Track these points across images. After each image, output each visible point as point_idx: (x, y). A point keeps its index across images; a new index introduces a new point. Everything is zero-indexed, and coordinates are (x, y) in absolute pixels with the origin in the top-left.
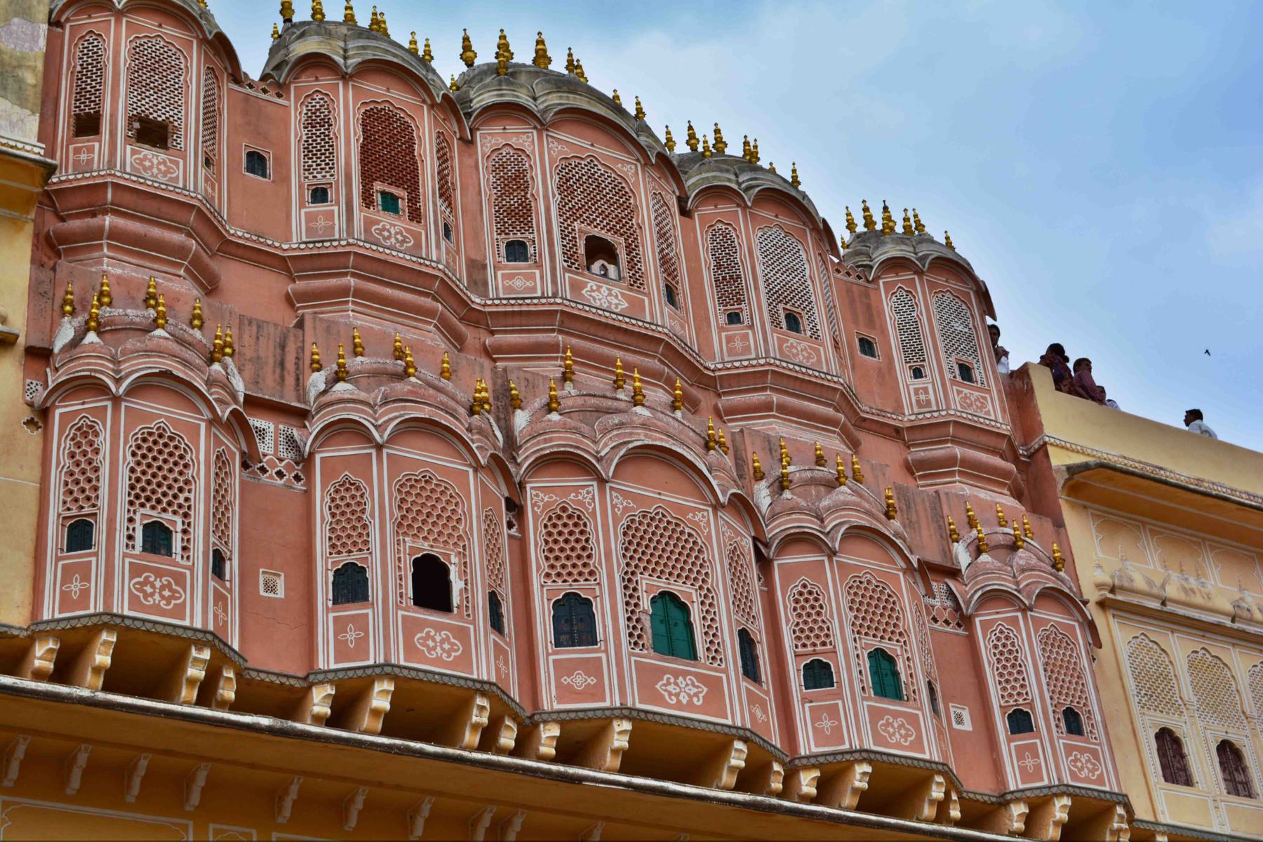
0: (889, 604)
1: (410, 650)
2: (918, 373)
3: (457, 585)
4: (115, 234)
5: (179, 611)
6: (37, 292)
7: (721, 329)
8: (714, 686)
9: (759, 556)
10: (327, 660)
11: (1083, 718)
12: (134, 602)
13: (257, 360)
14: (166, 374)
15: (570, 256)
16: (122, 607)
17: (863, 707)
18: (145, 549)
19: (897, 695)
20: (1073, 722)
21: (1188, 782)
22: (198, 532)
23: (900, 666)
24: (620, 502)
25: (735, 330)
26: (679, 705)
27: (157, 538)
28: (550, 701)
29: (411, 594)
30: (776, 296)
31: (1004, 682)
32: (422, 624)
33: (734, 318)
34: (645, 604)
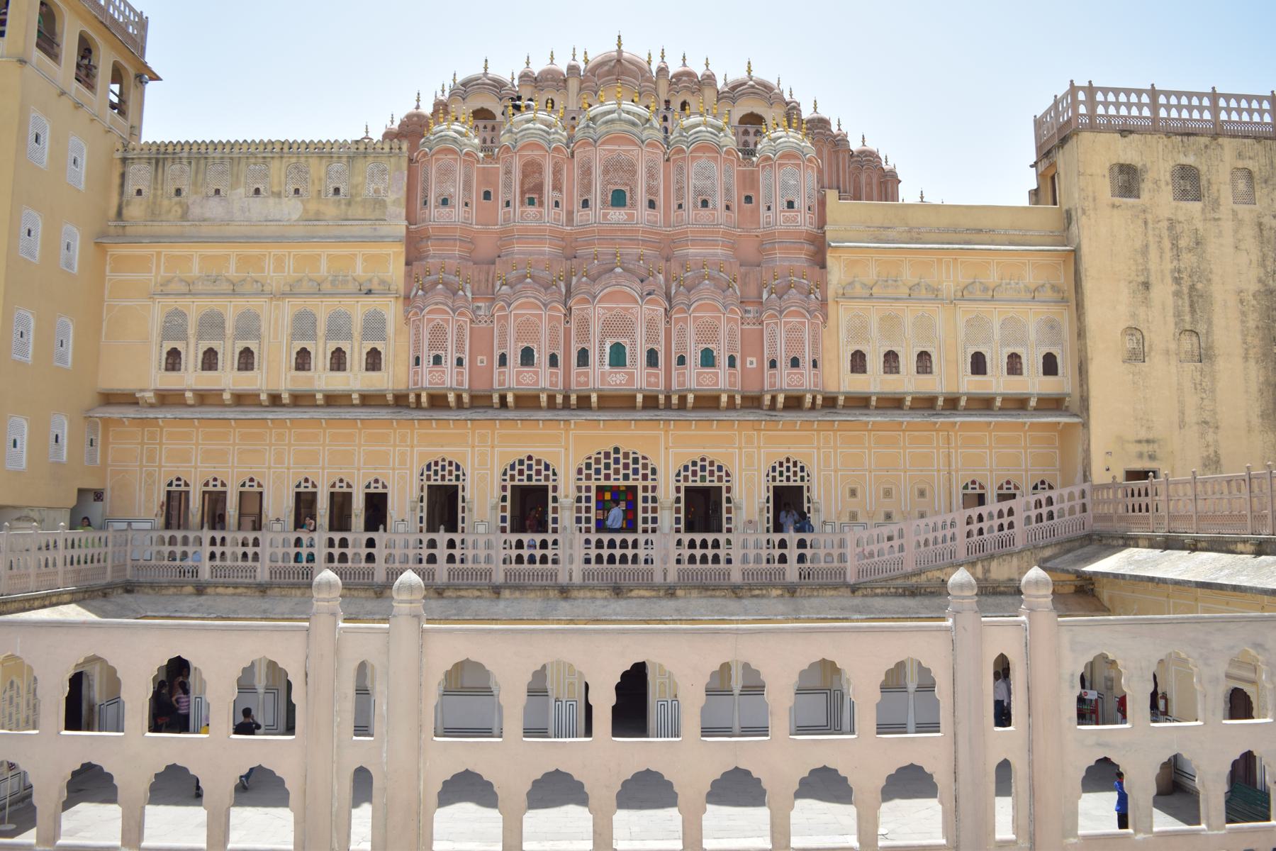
0: (715, 329)
1: (518, 382)
2: (769, 208)
3: (536, 355)
5: (443, 383)
6: (408, 275)
8: (631, 375)
10: (496, 386)
12: (430, 383)
13: (479, 281)
15: (604, 202)
17: (694, 376)
19: (713, 365)
20: (795, 363)
21: (865, 372)
24: (602, 311)
25: (680, 211)
27: (437, 360)
28: (574, 386)
30: (699, 192)
31: (770, 347)
33: (680, 206)
34: (608, 350)
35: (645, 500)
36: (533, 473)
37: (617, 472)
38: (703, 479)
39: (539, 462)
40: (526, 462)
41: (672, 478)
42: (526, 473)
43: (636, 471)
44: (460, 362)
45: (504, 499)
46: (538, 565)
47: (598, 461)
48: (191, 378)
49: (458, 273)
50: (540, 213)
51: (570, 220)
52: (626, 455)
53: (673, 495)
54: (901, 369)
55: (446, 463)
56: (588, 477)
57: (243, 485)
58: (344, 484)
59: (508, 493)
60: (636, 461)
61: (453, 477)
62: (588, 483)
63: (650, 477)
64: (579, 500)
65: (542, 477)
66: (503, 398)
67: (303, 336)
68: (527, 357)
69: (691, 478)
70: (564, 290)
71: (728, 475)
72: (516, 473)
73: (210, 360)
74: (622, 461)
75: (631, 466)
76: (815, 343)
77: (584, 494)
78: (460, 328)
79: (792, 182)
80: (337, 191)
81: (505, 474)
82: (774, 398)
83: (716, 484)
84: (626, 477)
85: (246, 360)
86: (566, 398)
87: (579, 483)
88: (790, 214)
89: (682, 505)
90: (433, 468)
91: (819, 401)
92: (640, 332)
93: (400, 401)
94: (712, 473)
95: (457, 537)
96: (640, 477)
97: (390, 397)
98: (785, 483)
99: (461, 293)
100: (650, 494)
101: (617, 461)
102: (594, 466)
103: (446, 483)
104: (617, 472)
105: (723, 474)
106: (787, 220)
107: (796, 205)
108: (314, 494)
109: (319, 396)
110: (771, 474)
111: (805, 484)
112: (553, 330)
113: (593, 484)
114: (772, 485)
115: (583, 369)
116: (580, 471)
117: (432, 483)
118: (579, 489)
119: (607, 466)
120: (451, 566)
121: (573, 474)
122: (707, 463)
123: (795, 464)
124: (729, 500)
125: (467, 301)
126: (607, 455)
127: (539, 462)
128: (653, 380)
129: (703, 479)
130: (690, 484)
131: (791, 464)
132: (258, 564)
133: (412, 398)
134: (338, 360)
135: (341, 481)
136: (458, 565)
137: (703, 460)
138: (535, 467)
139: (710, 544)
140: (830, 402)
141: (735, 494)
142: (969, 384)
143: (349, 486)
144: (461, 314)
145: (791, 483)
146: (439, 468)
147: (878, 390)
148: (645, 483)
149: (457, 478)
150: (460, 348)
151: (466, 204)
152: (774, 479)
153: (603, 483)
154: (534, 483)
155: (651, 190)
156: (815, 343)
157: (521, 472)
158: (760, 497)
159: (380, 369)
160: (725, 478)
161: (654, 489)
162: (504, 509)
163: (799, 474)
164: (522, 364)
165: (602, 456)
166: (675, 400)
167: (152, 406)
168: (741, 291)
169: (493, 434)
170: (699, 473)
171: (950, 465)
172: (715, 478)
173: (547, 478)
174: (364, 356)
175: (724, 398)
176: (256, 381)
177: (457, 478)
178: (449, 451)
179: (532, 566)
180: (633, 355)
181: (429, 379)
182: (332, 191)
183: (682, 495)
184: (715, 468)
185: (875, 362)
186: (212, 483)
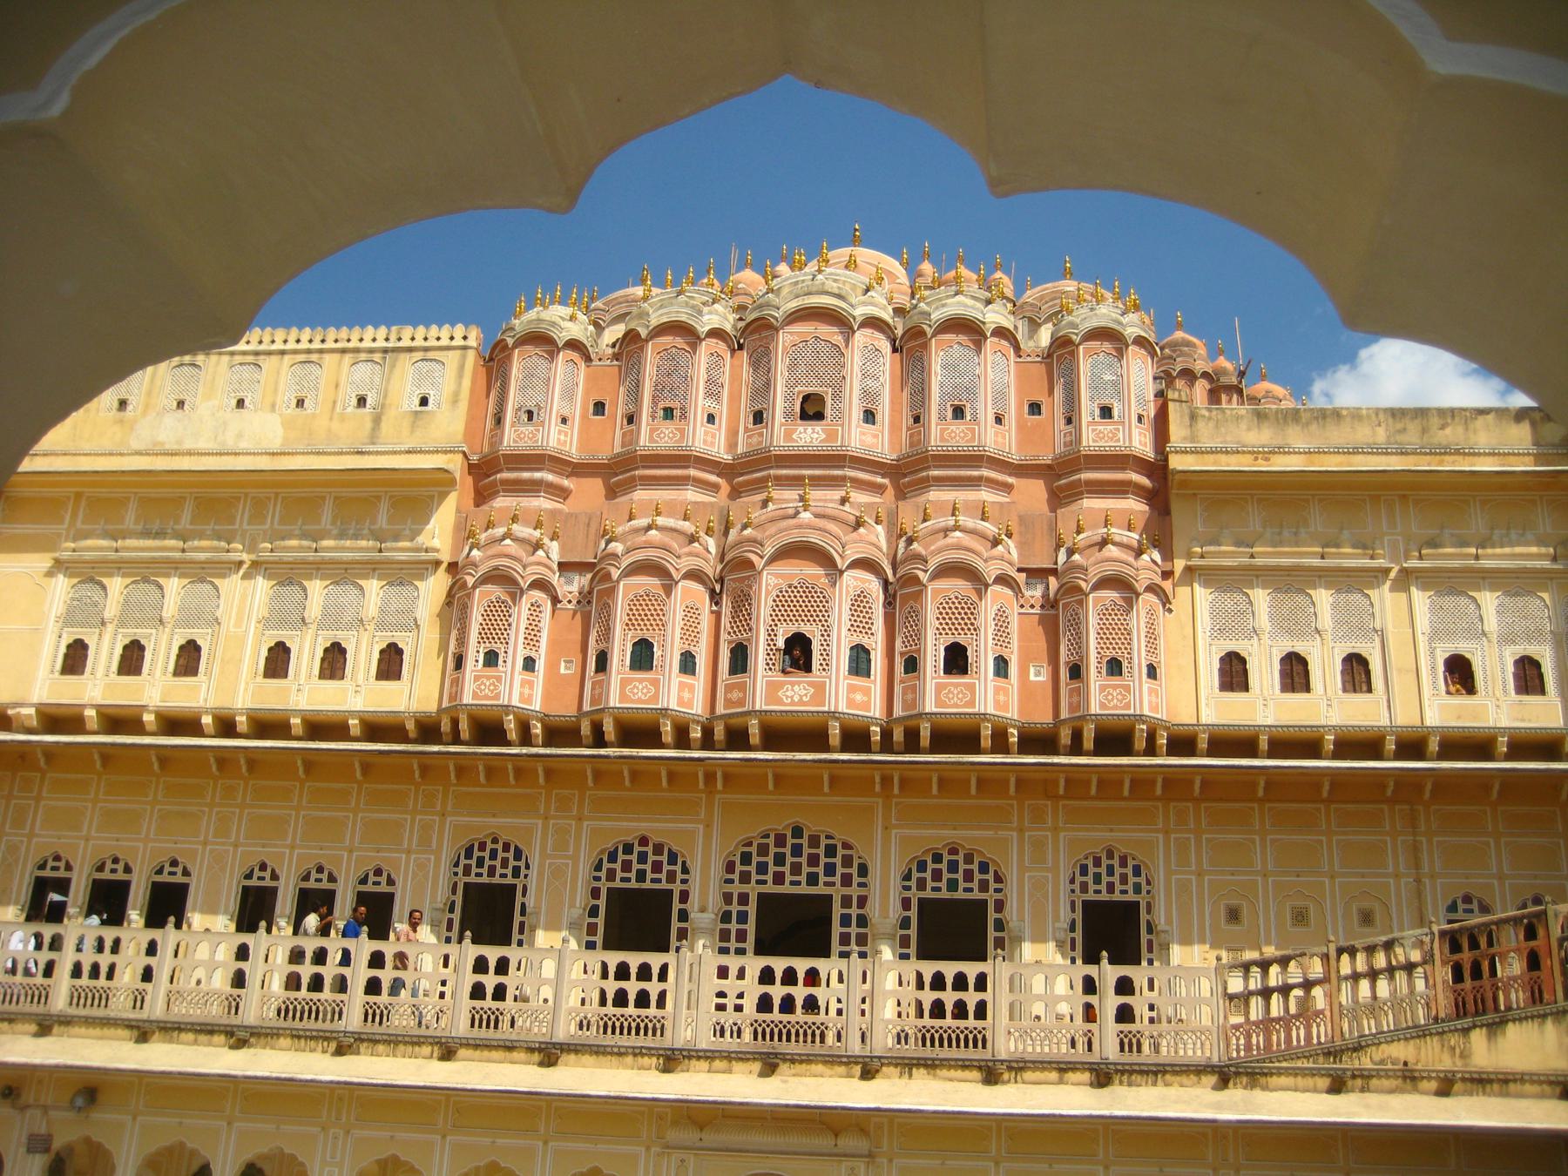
2: (1069, 421)
3: (657, 652)
4: (504, 482)
5: (497, 697)
7: (908, 429)
8: (820, 688)
9: (886, 590)
10: (587, 707)
11: (1125, 664)
12: (475, 695)
14: (496, 568)
15: (788, 414)
16: (467, 699)
18: (484, 665)
19: (964, 670)
20: (1115, 667)
21: (1246, 688)
22: (510, 652)
23: (969, 653)
26: (793, 703)
27: (491, 659)
28: (720, 709)
29: (628, 662)
32: (630, 681)
33: (917, 419)
34: (781, 644)
35: (846, 921)
36: (648, 867)
37: (796, 869)
38: (952, 885)
39: (658, 849)
40: (637, 849)
41: (895, 881)
42: (636, 866)
43: (830, 870)
44: (529, 664)
45: (594, 912)
46: (631, 1010)
47: (763, 850)
48: (98, 687)
49: (539, 525)
50: (682, 431)
51: (732, 445)
52: (814, 841)
53: (895, 911)
54: (1312, 685)
55: (500, 847)
56: (745, 877)
57: (160, 872)
58: (324, 876)
59: (602, 903)
60: (831, 851)
61: (509, 871)
62: (745, 888)
63: (856, 880)
64: (726, 917)
65: (663, 876)
66: (598, 729)
67: (282, 623)
68: (643, 655)
69: (930, 884)
70: (713, 550)
71: (998, 879)
72: (618, 866)
73: (132, 659)
74: (806, 851)
75: (823, 860)
76: (1152, 637)
77: (735, 908)
78: (535, 605)
79: (1108, 377)
80: (362, 401)
81: (598, 868)
82: (1077, 736)
83: (976, 895)
84: (813, 880)
85: (189, 659)
86: (708, 732)
87: (728, 888)
88: (1106, 428)
89: (913, 932)
90: (476, 854)
91: (1162, 741)
92: (841, 613)
93: (428, 730)
94: (969, 876)
95: (493, 954)
96: (837, 879)
97: (410, 726)
98: (1105, 896)
99: (540, 553)
100: (854, 911)
101: (797, 850)
102: (755, 859)
103: (497, 880)
104: (796, 869)
105: (990, 877)
106: (1099, 434)
107: (1116, 413)
108: (274, 890)
109: (295, 721)
110: (1079, 879)
111: (1142, 900)
112: (691, 612)
113: (753, 890)
114: (1080, 898)
115: (738, 679)
116: (730, 867)
117: (472, 879)
118: (728, 898)
119: (780, 859)
120: (478, 1004)
121: (716, 870)
122: (960, 858)
123: (1123, 863)
124: (1000, 925)
125: (550, 568)
126: (780, 840)
127: (658, 849)
128: (859, 697)
129: (952, 885)
130: (928, 894)
131: (1116, 862)
132: (148, 986)
133: (446, 726)
134: (334, 661)
135: (320, 870)
136: (488, 1003)
137: (953, 851)
138: (651, 858)
139: (949, 981)
140: (1183, 743)
141: (1011, 913)
142: (1440, 710)
143: (332, 879)
144: (541, 585)
145: (1117, 897)
146: (486, 854)
147: (1269, 722)
148: (846, 891)
149: (516, 872)
150: (532, 639)
151: (564, 421)
152: (1084, 888)
153: (770, 888)
154: (648, 885)
155: (866, 394)
156: (1152, 637)
157: (627, 866)
158: (1056, 918)
159: (397, 676)
160: (993, 885)
161: (862, 901)
162: (592, 929)
163: (1132, 880)
164: (632, 667)
165: (771, 841)
166: (898, 735)
167: (30, 731)
168: (1020, 555)
169: (582, 800)
170: (946, 876)
171: (1417, 866)
172: (975, 885)
173: (671, 877)
174: (376, 656)
175: (986, 732)
176: (200, 695)
177: (516, 872)
178: (505, 824)
179: (619, 1011)
180: (826, 654)
181: (475, 690)
182: (354, 401)
183: (913, 914)
184: (975, 867)
185: (1264, 671)
186: (109, 866)
